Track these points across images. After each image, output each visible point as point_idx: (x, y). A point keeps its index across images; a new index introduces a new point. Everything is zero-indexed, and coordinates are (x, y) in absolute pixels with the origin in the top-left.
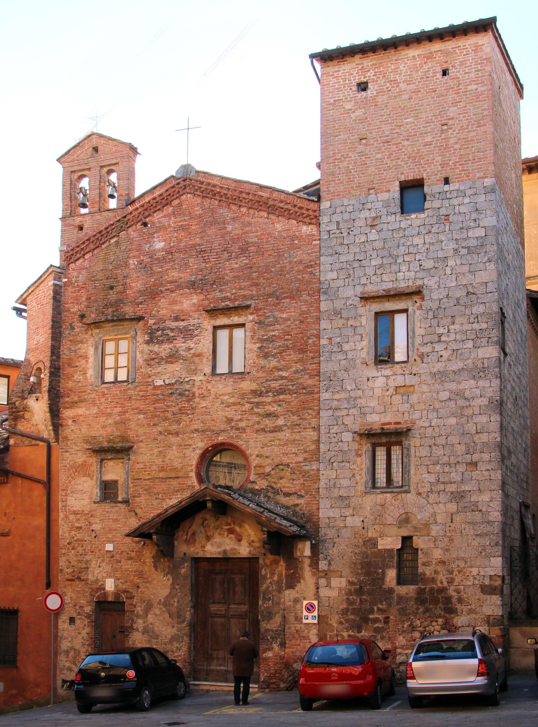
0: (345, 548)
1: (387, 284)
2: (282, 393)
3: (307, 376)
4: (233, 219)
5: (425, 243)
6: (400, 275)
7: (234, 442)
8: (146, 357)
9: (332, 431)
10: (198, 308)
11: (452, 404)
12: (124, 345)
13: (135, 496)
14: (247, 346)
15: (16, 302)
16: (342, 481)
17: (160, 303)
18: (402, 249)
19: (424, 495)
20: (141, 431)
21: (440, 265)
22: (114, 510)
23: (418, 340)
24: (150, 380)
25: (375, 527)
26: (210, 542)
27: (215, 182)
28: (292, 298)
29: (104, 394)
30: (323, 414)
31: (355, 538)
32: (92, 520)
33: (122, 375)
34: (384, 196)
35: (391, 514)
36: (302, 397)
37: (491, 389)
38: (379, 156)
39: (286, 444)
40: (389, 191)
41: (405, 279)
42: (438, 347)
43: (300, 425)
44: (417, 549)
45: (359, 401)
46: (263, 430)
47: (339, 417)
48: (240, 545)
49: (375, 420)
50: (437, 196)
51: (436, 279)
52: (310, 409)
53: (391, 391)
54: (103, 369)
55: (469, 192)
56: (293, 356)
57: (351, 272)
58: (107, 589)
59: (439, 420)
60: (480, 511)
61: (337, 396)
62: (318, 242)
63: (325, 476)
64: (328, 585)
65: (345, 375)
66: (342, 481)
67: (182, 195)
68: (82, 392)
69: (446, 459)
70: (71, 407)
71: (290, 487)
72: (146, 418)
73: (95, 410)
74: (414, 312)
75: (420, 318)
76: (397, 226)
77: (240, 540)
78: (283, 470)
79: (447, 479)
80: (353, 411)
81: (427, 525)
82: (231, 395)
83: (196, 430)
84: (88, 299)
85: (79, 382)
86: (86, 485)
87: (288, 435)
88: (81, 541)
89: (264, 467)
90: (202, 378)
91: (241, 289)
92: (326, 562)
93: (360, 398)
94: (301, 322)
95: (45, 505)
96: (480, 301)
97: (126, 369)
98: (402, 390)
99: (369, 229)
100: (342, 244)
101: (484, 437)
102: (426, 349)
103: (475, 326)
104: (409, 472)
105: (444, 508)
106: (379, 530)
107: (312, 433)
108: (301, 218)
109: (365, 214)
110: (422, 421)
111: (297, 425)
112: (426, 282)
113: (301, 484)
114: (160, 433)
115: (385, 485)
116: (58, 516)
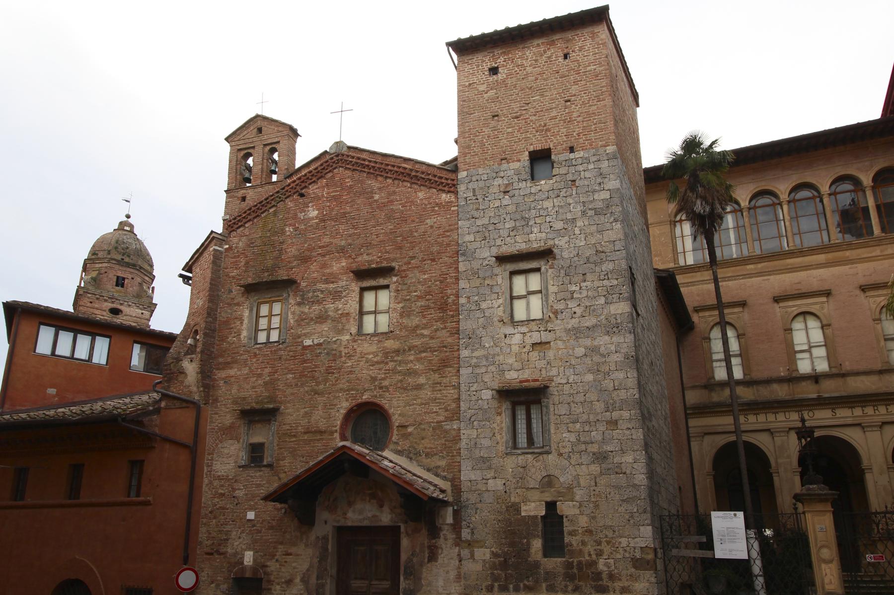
1: (519, 245)
2: (424, 352)
11: (588, 360)
12: (277, 308)
15: (183, 269)
18: (533, 211)
23: (552, 298)
24: (300, 340)
25: (518, 491)
29: (255, 355)
31: (498, 503)
33: (274, 336)
34: (516, 165)
35: (534, 477)
38: (510, 130)
39: (428, 403)
40: (519, 161)
41: (536, 239)
43: (440, 383)
45: (497, 358)
46: (405, 389)
47: (478, 374)
51: (566, 238)
53: (528, 347)
54: (257, 330)
56: (434, 314)
57: (487, 235)
58: (245, 563)
59: (576, 377)
61: (476, 354)
62: (456, 208)
63: (466, 436)
64: (472, 556)
65: (484, 333)
70: (223, 369)
71: (431, 448)
72: (293, 378)
73: (246, 371)
74: (547, 271)
82: (375, 354)
83: (341, 389)
86: (232, 448)
89: (406, 427)
93: (498, 355)
94: (441, 282)
97: (278, 331)
98: (538, 347)
102: (560, 306)
104: (549, 431)
105: (587, 470)
106: (521, 494)
107: (452, 392)
109: (499, 181)
111: (438, 383)
112: (557, 243)
115: (526, 445)
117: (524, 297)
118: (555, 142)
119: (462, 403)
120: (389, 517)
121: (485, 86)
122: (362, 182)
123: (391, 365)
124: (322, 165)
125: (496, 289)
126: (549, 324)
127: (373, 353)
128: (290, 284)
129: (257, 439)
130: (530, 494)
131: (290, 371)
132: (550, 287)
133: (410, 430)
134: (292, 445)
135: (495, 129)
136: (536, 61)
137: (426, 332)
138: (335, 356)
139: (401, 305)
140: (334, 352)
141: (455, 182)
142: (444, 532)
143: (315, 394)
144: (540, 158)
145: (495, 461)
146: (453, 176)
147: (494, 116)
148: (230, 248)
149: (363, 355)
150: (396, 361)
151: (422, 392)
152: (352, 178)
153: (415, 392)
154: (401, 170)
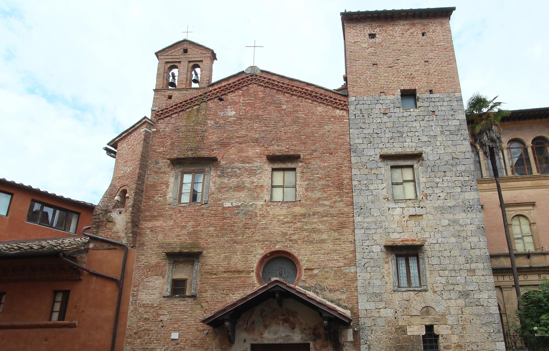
0: (381, 334)
1: (396, 149)
2: (326, 216)
3: (344, 205)
4: (287, 102)
5: (420, 126)
6: (406, 144)
7: (288, 250)
8: (217, 186)
9: (364, 244)
10: (260, 156)
13: (201, 292)
14: (297, 183)
16: (375, 281)
17: (230, 150)
19: (439, 293)
20: (210, 240)
21: (432, 140)
22: (182, 303)
23: (422, 185)
24: (220, 202)
25: (404, 317)
27: (274, 78)
28: (331, 154)
29: (180, 211)
30: (356, 231)
32: (161, 312)
34: (392, 97)
36: (341, 219)
37: (477, 220)
40: (394, 95)
42: (436, 191)
43: (340, 239)
44: (437, 336)
45: (383, 224)
46: (311, 242)
48: (294, 333)
49: (398, 237)
50: (426, 100)
51: (431, 148)
52: (347, 228)
53: (407, 218)
54: (181, 193)
55: (448, 99)
57: (372, 140)
59: (443, 240)
60: (482, 306)
65: (372, 206)
66: (375, 281)
67: (250, 84)
68: (161, 209)
69: (451, 267)
70: (150, 220)
72: (216, 230)
73: (171, 223)
75: (422, 171)
76: (401, 115)
77: (293, 328)
78: (328, 272)
79: (454, 282)
80: (380, 231)
81: (443, 315)
82: (285, 216)
83: (257, 241)
84: (172, 144)
85: (159, 201)
86: (157, 282)
87: (331, 246)
88: (148, 330)
89: (311, 269)
90: (262, 203)
91: (293, 145)
92: (366, 346)
95: (116, 299)
96: (462, 163)
98: (414, 218)
99: (382, 116)
100: (364, 123)
101: (477, 252)
102: (429, 191)
103: (460, 178)
107: (349, 246)
108: (335, 105)
109: (379, 106)
110: (431, 239)
111: (337, 239)
112: (424, 150)
113: (343, 283)
114: (227, 241)
116: (128, 309)
117: (401, 184)
118: (420, 86)
119: (357, 254)
120: (300, 336)
121: (366, 45)
122: (272, 96)
123: (299, 225)
124: (238, 81)
125: (380, 177)
126: (421, 203)
127: (284, 215)
128: (212, 161)
129: (179, 276)
130: (413, 320)
131: (211, 225)
132: (421, 178)
133: (315, 272)
134: (214, 281)
135: (374, 72)
136: (402, 34)
137: (326, 203)
138: (251, 216)
139: (306, 183)
140: (250, 213)
141: (347, 103)
142: (346, 348)
143: (234, 242)
144: (409, 95)
145: (385, 296)
146: (345, 99)
147: (374, 64)
148: (158, 131)
149: (274, 216)
150: (303, 222)
151: (324, 245)
152: (264, 92)
153: (319, 245)
154: (304, 90)
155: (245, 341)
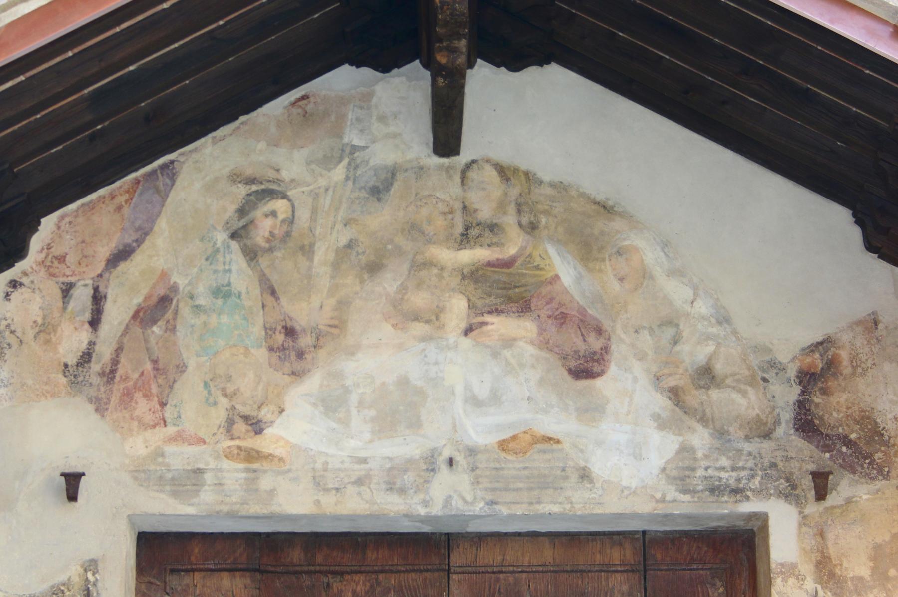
26: (313, 382)
48: (592, 411)
77: (586, 368)
155: (72, 484)
